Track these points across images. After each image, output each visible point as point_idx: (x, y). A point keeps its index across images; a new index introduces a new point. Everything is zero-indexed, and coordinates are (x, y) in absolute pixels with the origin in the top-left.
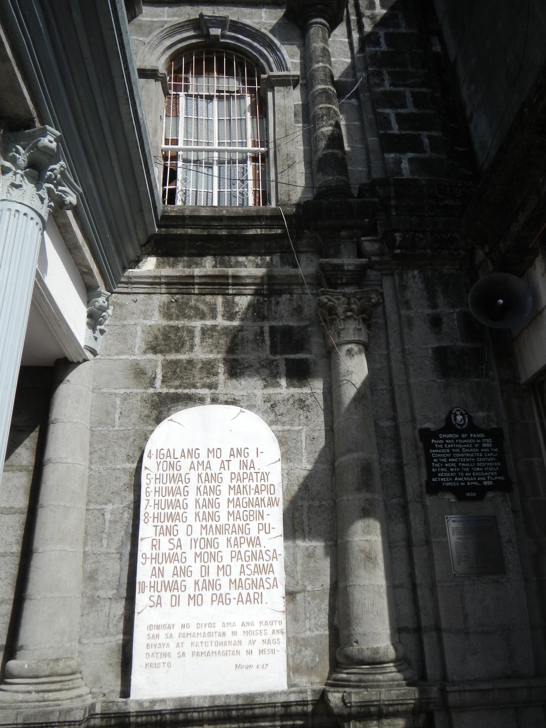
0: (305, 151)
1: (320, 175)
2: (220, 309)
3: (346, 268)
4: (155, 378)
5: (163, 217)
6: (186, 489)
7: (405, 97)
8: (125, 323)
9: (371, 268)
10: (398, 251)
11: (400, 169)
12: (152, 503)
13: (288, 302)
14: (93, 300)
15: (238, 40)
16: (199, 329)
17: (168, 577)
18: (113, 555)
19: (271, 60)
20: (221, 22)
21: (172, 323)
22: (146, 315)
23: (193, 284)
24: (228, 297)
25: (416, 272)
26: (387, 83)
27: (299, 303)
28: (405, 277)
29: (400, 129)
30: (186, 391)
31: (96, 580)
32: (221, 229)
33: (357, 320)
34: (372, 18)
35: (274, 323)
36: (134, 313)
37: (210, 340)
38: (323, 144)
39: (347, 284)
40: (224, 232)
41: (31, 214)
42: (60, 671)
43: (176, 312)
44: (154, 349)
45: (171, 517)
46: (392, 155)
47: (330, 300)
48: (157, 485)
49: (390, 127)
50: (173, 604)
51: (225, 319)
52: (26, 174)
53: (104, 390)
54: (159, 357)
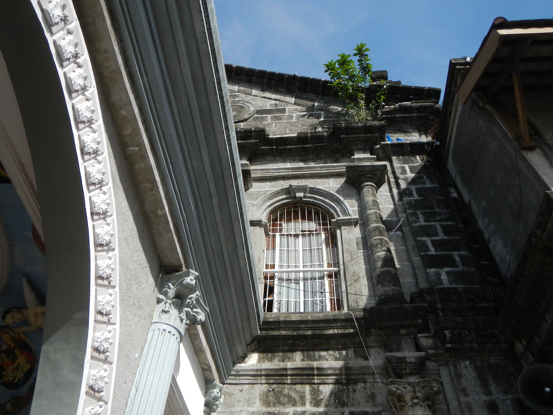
0: (366, 269)
1: (379, 287)
2: (308, 396)
3: (408, 360)
5: (264, 322)
7: (436, 229)
8: (233, 410)
9: (429, 360)
10: (449, 346)
11: (440, 279)
13: (363, 390)
14: (210, 391)
15: (315, 198)
19: (338, 209)
20: (303, 189)
21: (271, 410)
22: (249, 403)
23: (286, 375)
24: (314, 386)
25: (467, 363)
27: (372, 390)
28: (458, 367)
29: (436, 251)
32: (307, 330)
33: (423, 407)
34: (405, 179)
35: (353, 409)
36: (240, 401)
38: (379, 264)
39: (411, 374)
40: (309, 333)
41: (174, 331)
43: (273, 399)
46: (433, 270)
47: (398, 389)
49: (428, 250)
51: (312, 406)
52: (173, 303)
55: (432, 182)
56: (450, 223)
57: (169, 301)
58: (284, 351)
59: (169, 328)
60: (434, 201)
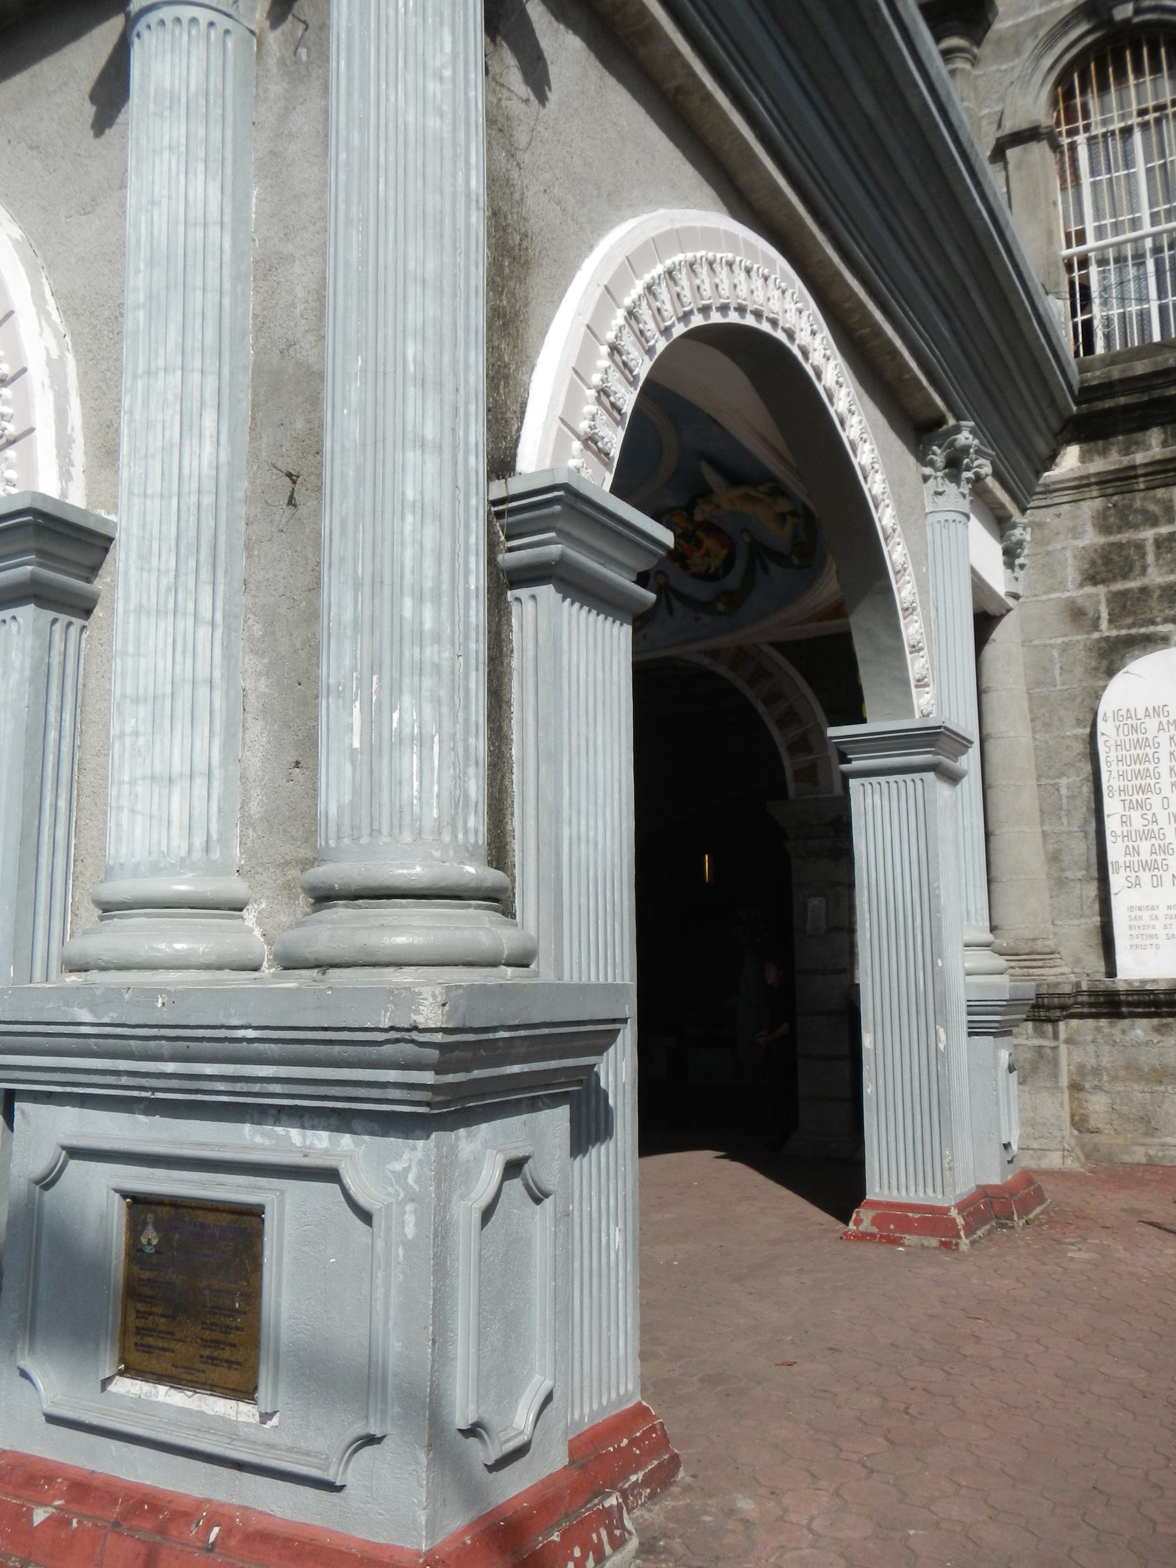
4: (1099, 618)
5: (1083, 390)
6: (1157, 786)
8: (1050, 548)
12: (1115, 774)
14: (1008, 533)
16: (1151, 541)
17: (1145, 855)
18: (1077, 834)
22: (1075, 533)
23: (1136, 477)
30: (1143, 630)
31: (1061, 861)
32: (1168, 386)
36: (1058, 533)
37: (1169, 555)
42: (1039, 950)
44: (1092, 578)
45: (1141, 789)
48: (1119, 753)
50: (1155, 884)
52: (947, 476)
53: (1036, 642)
54: (1101, 590)
57: (940, 474)
58: (1128, 431)
59: (951, 516)
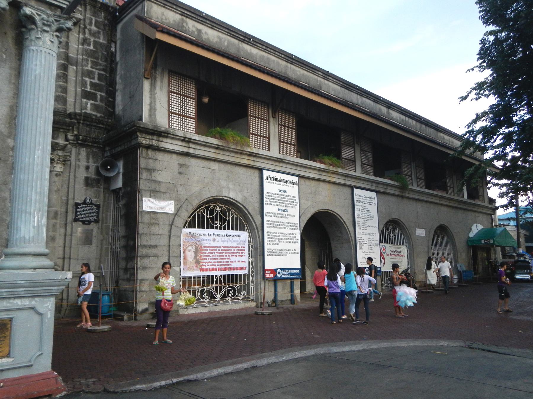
7: (95, 74)
11: (87, 106)
25: (84, 149)
26: (89, 66)
29: (90, 89)
34: (90, 30)
39: (60, 150)
46: (85, 100)
49: (86, 87)
55: (104, 40)
56: (103, 73)
60: (100, 54)
